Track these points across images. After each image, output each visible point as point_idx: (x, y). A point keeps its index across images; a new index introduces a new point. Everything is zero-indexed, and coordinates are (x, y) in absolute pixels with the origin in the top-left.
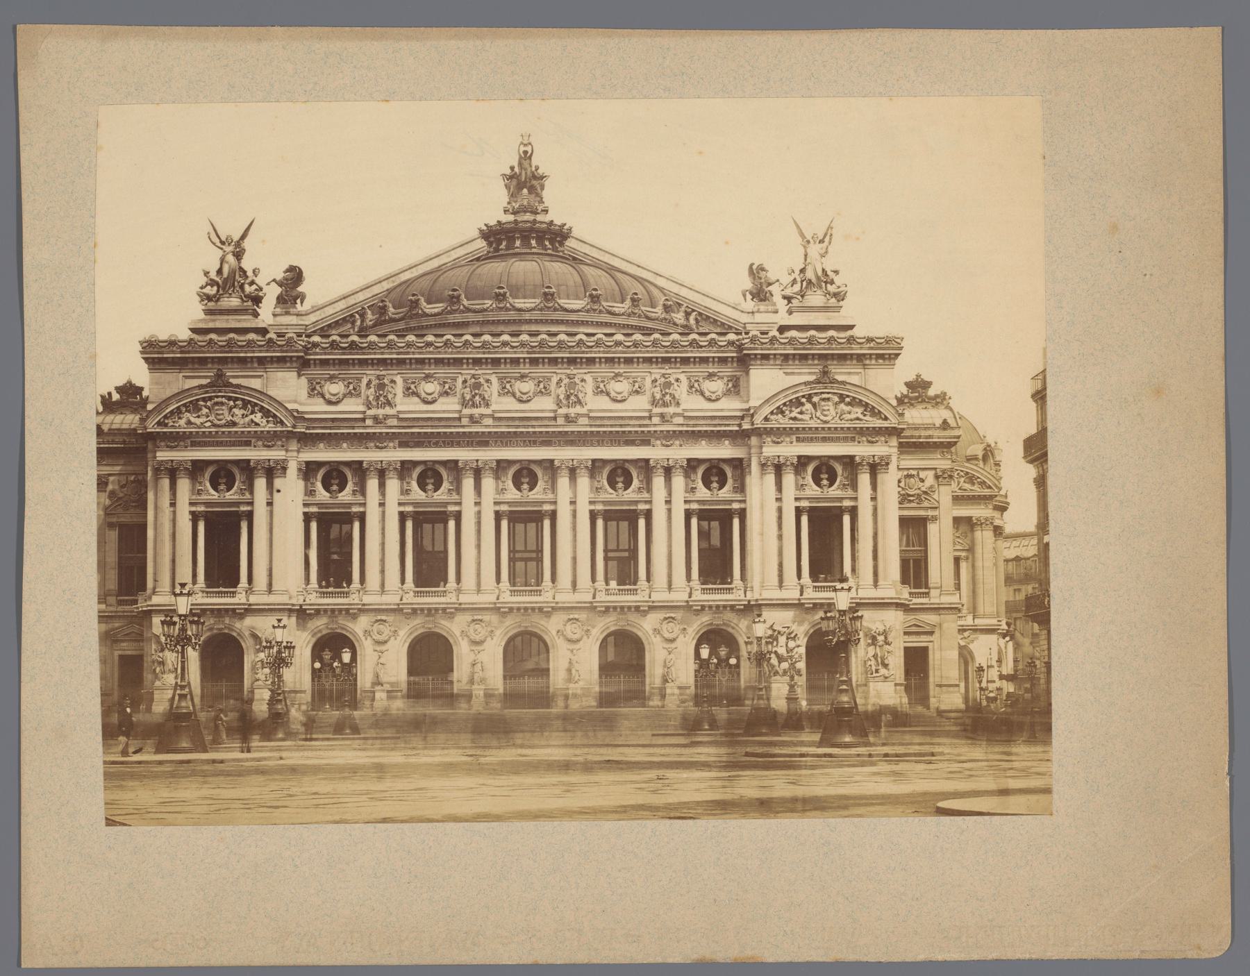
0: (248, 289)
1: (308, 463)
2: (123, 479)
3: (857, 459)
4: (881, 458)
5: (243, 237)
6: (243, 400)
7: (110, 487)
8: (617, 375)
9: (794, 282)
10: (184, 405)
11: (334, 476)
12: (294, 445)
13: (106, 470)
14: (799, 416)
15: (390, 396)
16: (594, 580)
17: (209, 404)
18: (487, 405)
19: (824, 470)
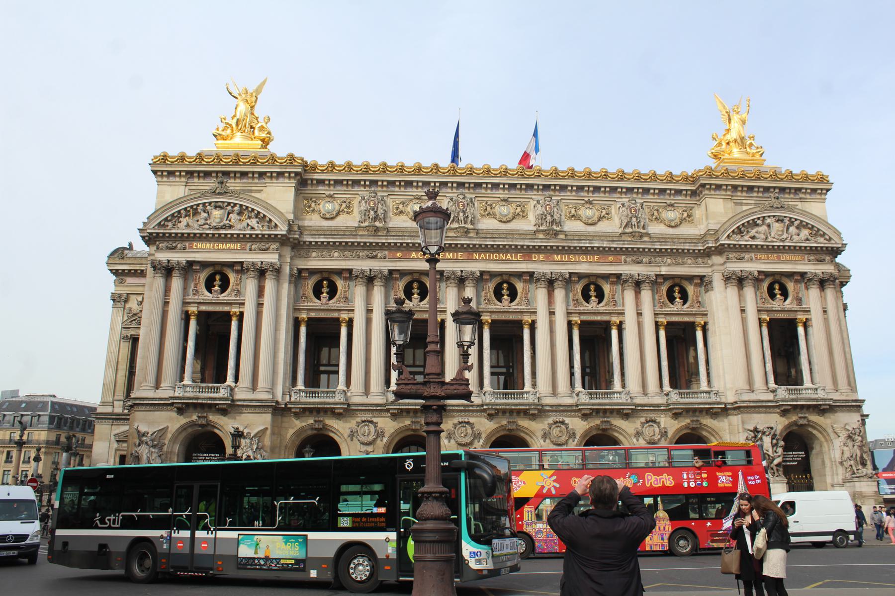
0: (256, 131)
1: (300, 271)
2: (140, 299)
3: (809, 275)
4: (831, 275)
5: (258, 91)
6: (241, 206)
7: (128, 306)
8: (590, 203)
9: (720, 144)
10: (185, 209)
11: (326, 284)
12: (287, 252)
13: (123, 290)
14: (757, 235)
15: (380, 212)
16: (572, 384)
17: (208, 208)
18: (472, 223)
19: (776, 285)
